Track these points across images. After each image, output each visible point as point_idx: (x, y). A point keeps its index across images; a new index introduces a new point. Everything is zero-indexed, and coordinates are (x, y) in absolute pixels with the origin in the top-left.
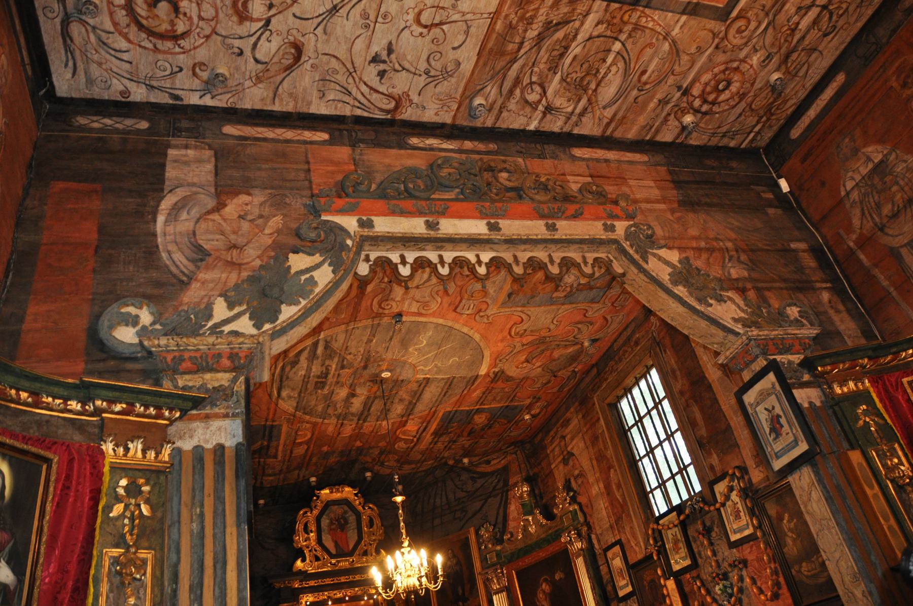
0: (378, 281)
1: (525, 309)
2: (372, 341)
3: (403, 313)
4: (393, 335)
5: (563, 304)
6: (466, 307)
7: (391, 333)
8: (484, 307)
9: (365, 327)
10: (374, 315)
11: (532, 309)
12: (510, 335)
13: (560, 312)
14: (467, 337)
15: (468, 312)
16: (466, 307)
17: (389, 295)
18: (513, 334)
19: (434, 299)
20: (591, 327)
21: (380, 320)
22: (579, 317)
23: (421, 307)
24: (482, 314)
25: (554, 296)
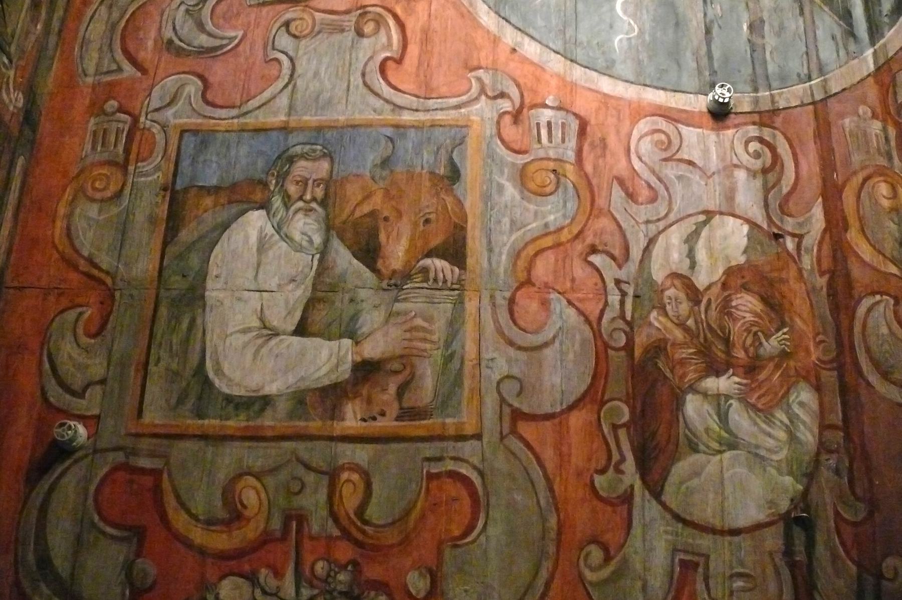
0: (807, 242)
1: (389, 116)
2: (751, 27)
4: (709, 44)
5: (285, 129)
6: (558, 134)
7: (716, 54)
8: (510, 131)
9: (784, 80)
10: (778, 121)
11: (371, 116)
12: (396, 17)
13: (283, 101)
14: (513, 20)
15: (546, 115)
16: (558, 134)
17: (767, 190)
18: (391, 22)
19: (653, 172)
20: (168, 33)
21: (756, 101)
22: (218, 71)
23: (676, 141)
24: (505, 105)
25: (325, 165)
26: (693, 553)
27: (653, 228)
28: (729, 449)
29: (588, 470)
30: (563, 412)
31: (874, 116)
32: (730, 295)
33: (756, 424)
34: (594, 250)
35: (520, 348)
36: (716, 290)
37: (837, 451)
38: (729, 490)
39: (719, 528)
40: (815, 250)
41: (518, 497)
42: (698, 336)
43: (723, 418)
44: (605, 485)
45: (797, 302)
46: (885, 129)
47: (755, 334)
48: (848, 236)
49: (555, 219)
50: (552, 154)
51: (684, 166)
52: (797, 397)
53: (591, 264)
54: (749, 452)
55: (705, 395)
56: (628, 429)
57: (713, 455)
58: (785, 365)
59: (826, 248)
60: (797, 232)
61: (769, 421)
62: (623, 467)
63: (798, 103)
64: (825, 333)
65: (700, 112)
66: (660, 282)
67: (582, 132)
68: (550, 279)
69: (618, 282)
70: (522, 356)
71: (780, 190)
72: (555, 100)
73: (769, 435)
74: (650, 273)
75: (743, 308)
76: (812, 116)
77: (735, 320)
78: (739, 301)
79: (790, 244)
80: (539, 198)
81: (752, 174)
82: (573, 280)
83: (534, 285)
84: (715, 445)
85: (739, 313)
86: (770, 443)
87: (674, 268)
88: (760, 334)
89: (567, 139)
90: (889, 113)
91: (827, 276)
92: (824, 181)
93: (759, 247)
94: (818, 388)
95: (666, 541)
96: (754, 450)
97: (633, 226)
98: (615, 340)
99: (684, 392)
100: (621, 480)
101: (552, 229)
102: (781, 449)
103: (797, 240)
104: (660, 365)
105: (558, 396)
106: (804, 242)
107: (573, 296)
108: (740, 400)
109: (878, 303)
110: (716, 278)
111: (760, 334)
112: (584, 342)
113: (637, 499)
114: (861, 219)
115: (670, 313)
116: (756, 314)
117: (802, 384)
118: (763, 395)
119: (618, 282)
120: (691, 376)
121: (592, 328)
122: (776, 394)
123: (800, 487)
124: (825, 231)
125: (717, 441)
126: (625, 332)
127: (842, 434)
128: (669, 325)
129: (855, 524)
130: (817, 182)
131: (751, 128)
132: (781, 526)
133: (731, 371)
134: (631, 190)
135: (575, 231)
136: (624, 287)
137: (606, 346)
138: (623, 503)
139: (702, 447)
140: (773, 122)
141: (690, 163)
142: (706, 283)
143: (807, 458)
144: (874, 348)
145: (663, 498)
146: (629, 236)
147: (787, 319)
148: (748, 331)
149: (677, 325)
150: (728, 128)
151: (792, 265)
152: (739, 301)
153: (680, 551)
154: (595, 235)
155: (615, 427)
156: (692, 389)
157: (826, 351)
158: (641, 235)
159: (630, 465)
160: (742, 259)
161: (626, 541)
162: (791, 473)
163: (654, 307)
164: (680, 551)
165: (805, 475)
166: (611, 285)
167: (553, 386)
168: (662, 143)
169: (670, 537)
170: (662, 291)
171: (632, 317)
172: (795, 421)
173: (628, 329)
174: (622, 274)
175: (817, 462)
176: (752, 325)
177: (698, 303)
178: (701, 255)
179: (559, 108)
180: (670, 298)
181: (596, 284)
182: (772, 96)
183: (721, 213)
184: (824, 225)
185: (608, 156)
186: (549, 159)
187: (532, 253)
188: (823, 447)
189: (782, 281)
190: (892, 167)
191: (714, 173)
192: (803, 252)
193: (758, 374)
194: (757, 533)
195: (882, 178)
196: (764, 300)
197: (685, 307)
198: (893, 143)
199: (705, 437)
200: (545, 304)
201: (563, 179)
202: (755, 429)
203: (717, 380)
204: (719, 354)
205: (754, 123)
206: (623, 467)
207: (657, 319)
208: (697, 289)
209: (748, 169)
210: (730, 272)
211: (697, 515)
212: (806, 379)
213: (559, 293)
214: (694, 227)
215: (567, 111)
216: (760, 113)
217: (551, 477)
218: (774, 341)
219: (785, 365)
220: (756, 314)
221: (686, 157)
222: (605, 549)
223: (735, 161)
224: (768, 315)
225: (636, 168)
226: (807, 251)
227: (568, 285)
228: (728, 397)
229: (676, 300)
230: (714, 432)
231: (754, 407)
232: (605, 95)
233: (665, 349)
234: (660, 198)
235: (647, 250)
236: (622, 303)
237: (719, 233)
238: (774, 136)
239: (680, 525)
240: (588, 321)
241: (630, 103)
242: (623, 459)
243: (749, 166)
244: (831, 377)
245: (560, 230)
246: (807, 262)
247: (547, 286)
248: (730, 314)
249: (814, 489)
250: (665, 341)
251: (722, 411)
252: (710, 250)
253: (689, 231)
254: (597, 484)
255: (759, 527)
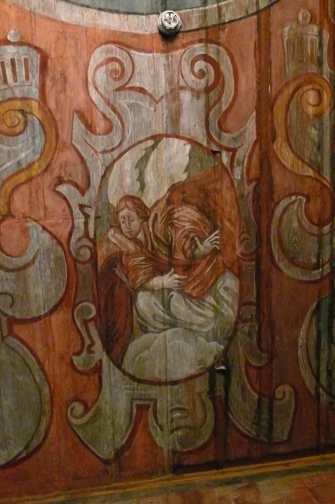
0: (239, 155)
3: (158, 43)
6: (21, 71)
10: (223, 36)
16: (21, 71)
17: (208, 108)
19: (108, 103)
21: (205, 15)
26: (145, 400)
27: (109, 157)
28: (171, 328)
29: (68, 353)
30: (46, 315)
31: (313, 21)
32: (173, 209)
33: (191, 308)
34: (60, 181)
35: (7, 270)
36: (162, 205)
37: (251, 320)
38: (170, 354)
39: (164, 381)
40: (246, 162)
41: (20, 378)
42: (147, 247)
43: (167, 306)
44: (81, 362)
45: (227, 209)
46: (320, 34)
47: (193, 239)
48: (275, 146)
49: (26, 156)
50: (18, 93)
51: (135, 94)
52: (223, 283)
53: (59, 194)
54: (185, 328)
55: (153, 291)
56: (96, 321)
57: (159, 333)
58: (215, 261)
59: (255, 159)
60: (232, 146)
61: (201, 306)
62: (93, 349)
63: (243, 14)
64: (248, 232)
65: (152, 34)
66: (115, 205)
67: (44, 66)
68: (26, 209)
69: (82, 207)
70: (11, 276)
71: (221, 107)
72: (15, 35)
73: (201, 315)
74: (107, 198)
75: (184, 219)
76: (254, 27)
77: (177, 229)
78: (181, 213)
79: (225, 158)
80: (11, 138)
81: (196, 94)
82: (46, 208)
83: (14, 217)
84: (161, 326)
85: (180, 223)
86: (201, 320)
87: (127, 191)
88: (196, 238)
89: (30, 75)
90: (327, 16)
91: (254, 184)
92: (259, 93)
93: (199, 164)
94: (240, 276)
95: (126, 394)
96: (188, 327)
97: (93, 156)
98: (81, 256)
99: (137, 291)
100: (93, 358)
101: (24, 165)
102: (209, 324)
103: (231, 153)
104: (117, 272)
105: (42, 303)
106: (237, 155)
107: (47, 223)
108: (178, 291)
109: (293, 203)
110: (161, 196)
111: (196, 238)
112: (58, 259)
113: (105, 368)
114: (287, 129)
115: (125, 230)
116: (193, 223)
117: (228, 274)
118: (197, 286)
119: (82, 207)
120: (141, 278)
121: (63, 248)
122: (207, 284)
123: (222, 347)
124: (256, 142)
125: (162, 323)
126: (89, 248)
127: (255, 308)
128: (123, 239)
129: (259, 368)
130: (253, 96)
131: (197, 46)
132: (207, 375)
133: (173, 270)
134: (90, 122)
135: (44, 166)
136: (87, 210)
137: (75, 261)
138: (95, 372)
139: (150, 329)
140: (219, 38)
141: (141, 90)
142: (154, 201)
143: (229, 327)
144: (286, 241)
145: (123, 367)
146: (89, 165)
147: (219, 223)
148: (187, 237)
149: (130, 239)
150: (177, 48)
151: (225, 176)
152: (181, 213)
153: (136, 399)
154: (61, 166)
155: (85, 322)
156: (143, 288)
157: (248, 246)
158: (99, 164)
159: (98, 346)
160: (183, 177)
161: (98, 397)
162: (215, 339)
163: (111, 227)
164: (136, 399)
165: (226, 338)
166: (76, 210)
167: (36, 296)
168: (115, 71)
169: (129, 392)
170: (117, 213)
171: (95, 235)
172: (221, 301)
173: (91, 245)
174: (85, 200)
175: (235, 330)
176: (190, 232)
177: (146, 219)
178: (150, 177)
179: (20, 44)
180: (124, 218)
181: (64, 210)
182: (219, 9)
183: (168, 136)
184: (255, 138)
185: (68, 92)
186: (13, 99)
187: (9, 190)
188: (239, 318)
189: (215, 190)
190: (322, 73)
191: (162, 97)
192: (235, 164)
193: (194, 271)
194: (190, 382)
195: (310, 86)
196: (201, 210)
197: (136, 224)
198: (325, 49)
199: (152, 321)
200: (25, 231)
201: (29, 117)
202: (190, 312)
203: (161, 278)
204: (163, 257)
205: (201, 41)
206: (93, 349)
207: (113, 236)
208: (146, 207)
209: (192, 90)
210: (174, 188)
211: (147, 376)
212: (231, 270)
213: (35, 221)
214: (144, 152)
215: (29, 45)
216: (206, 28)
217: (42, 361)
218: (207, 243)
219: (215, 261)
220: (193, 223)
221: (137, 84)
222: (85, 404)
223: (182, 83)
224: (203, 222)
225: (94, 99)
226: (240, 163)
227: (42, 213)
228: (170, 290)
229: (129, 218)
230: (160, 316)
231: (190, 296)
232: (62, 23)
233: (121, 260)
234: (114, 129)
235: (104, 177)
236: (86, 224)
237: (165, 155)
238: (218, 52)
239: (136, 383)
240: (59, 242)
241: (86, 30)
242: (93, 343)
243: (194, 87)
244: (249, 266)
245: (30, 166)
246: (238, 173)
247: (25, 217)
248: (172, 225)
249: (232, 348)
250: (121, 253)
251: (166, 300)
252: (157, 170)
253: (140, 157)
254: (75, 363)
255: (191, 378)
